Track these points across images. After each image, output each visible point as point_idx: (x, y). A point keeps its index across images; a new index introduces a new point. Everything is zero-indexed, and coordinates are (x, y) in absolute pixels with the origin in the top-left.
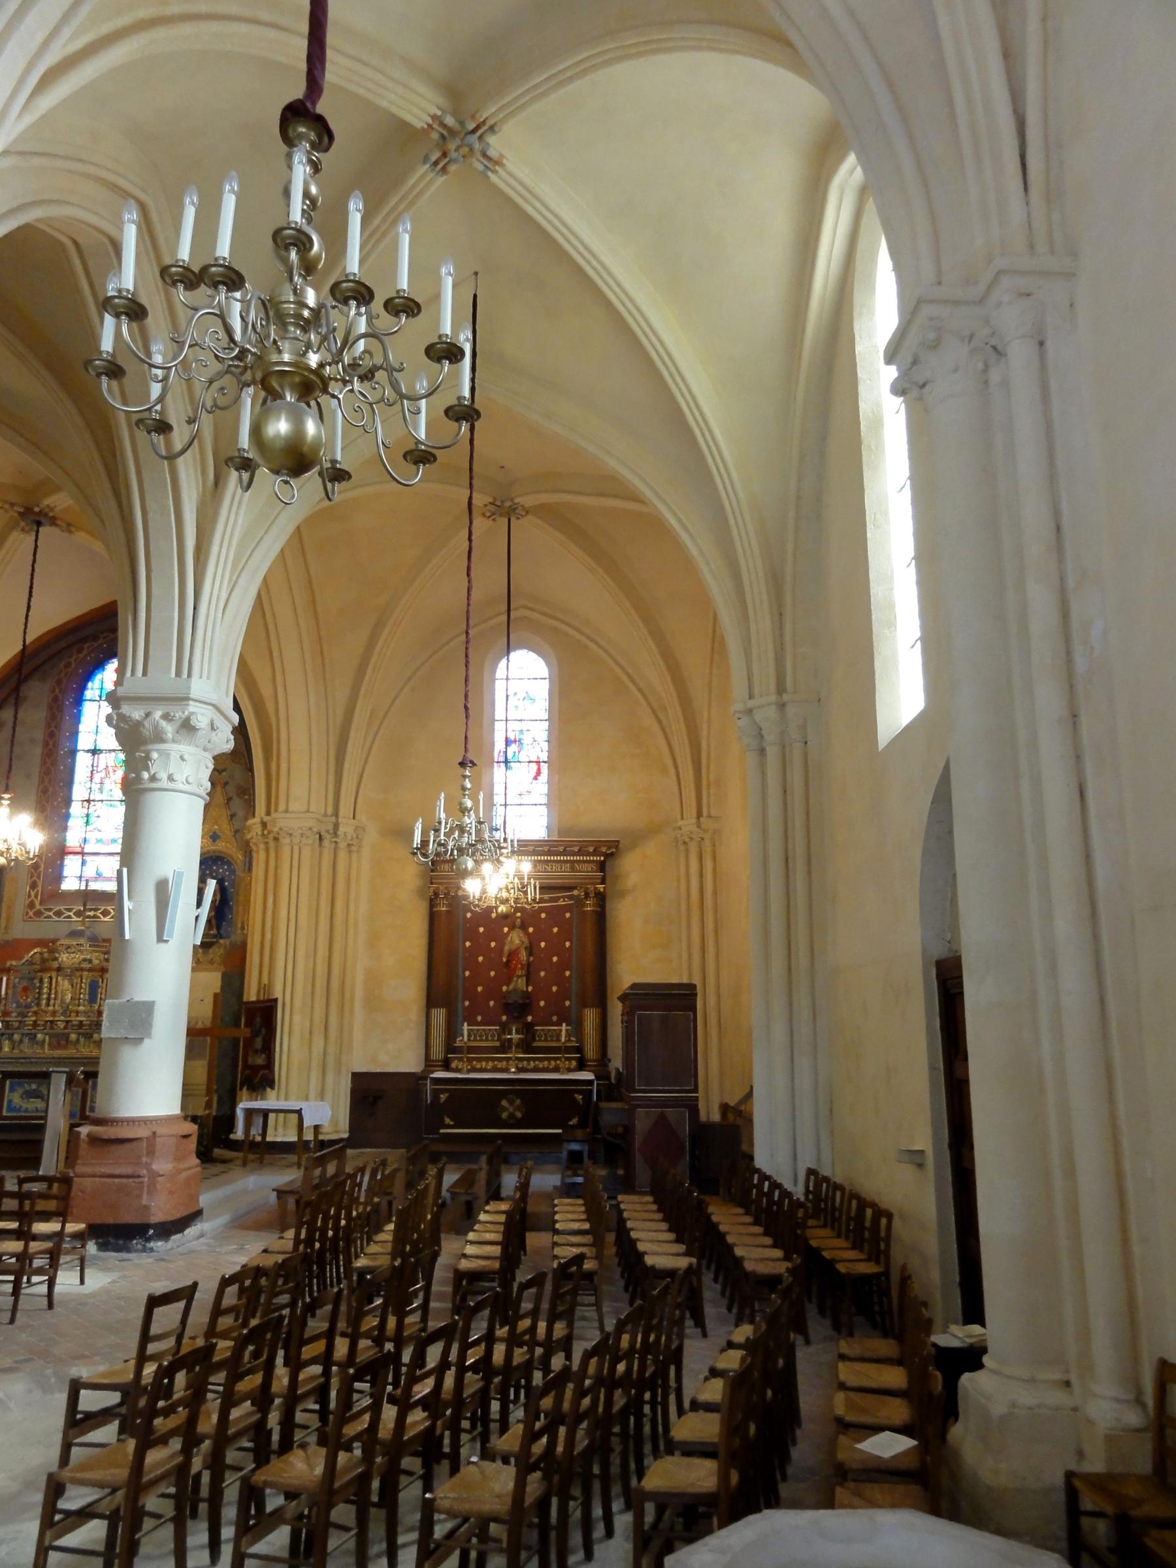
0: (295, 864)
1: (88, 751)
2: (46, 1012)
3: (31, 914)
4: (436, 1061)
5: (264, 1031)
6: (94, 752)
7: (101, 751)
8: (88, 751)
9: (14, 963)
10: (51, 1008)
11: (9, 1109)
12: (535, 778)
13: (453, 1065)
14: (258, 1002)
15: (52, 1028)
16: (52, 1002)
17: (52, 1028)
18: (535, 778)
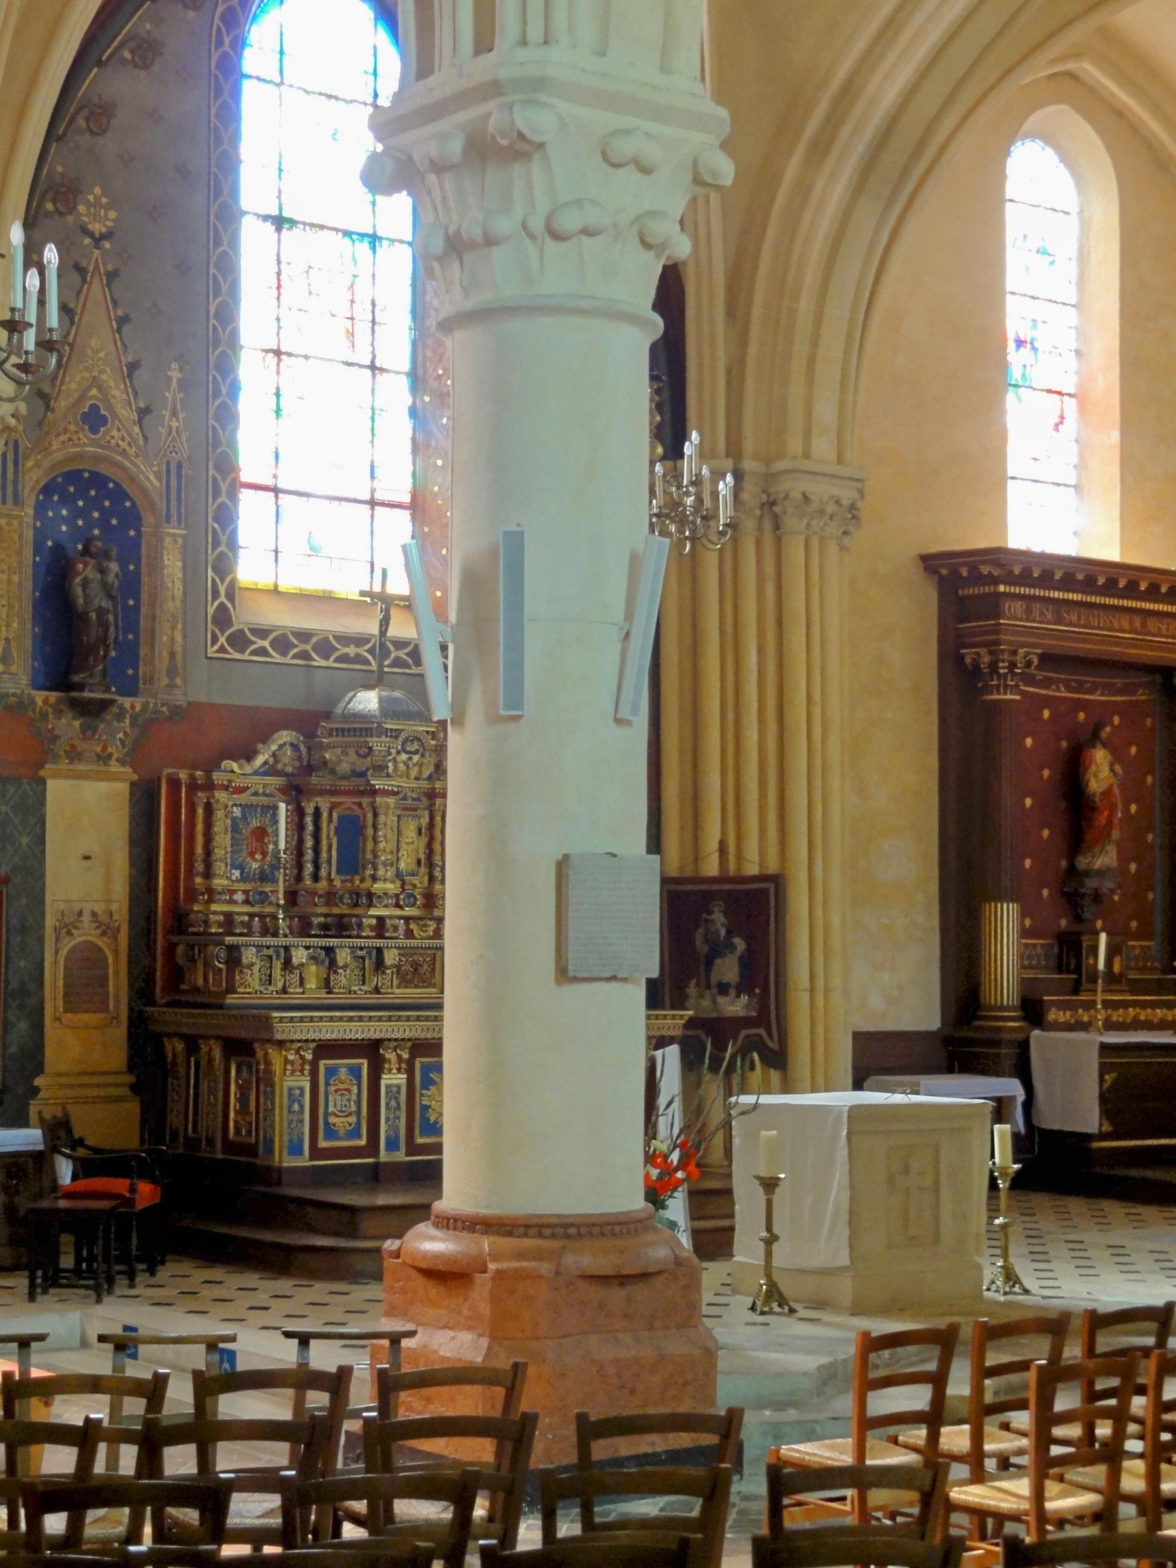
0: (815, 577)
1: (266, 218)
2: (314, 893)
3: (222, 640)
4: (1007, 1009)
5: (740, 944)
6: (280, 222)
7: (293, 223)
8: (266, 218)
9: (235, 766)
10: (323, 885)
11: (356, 1133)
12: (1056, 427)
13: (1053, 1015)
14: (723, 879)
15: (409, 934)
16: (323, 873)
17: (409, 934)
18: (1056, 427)
